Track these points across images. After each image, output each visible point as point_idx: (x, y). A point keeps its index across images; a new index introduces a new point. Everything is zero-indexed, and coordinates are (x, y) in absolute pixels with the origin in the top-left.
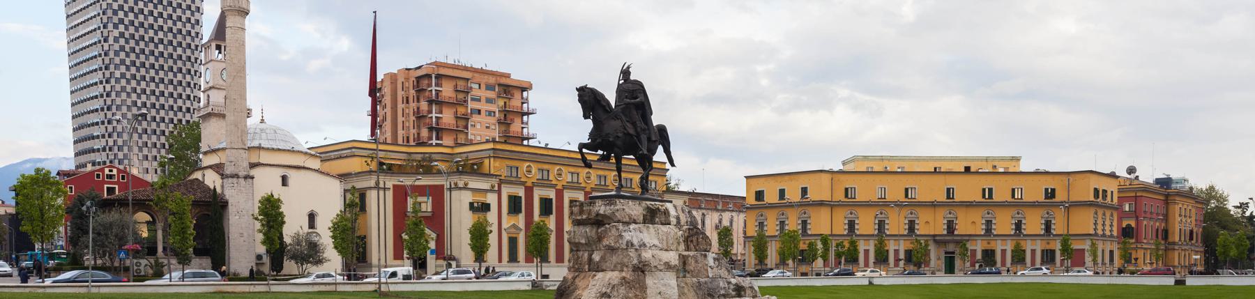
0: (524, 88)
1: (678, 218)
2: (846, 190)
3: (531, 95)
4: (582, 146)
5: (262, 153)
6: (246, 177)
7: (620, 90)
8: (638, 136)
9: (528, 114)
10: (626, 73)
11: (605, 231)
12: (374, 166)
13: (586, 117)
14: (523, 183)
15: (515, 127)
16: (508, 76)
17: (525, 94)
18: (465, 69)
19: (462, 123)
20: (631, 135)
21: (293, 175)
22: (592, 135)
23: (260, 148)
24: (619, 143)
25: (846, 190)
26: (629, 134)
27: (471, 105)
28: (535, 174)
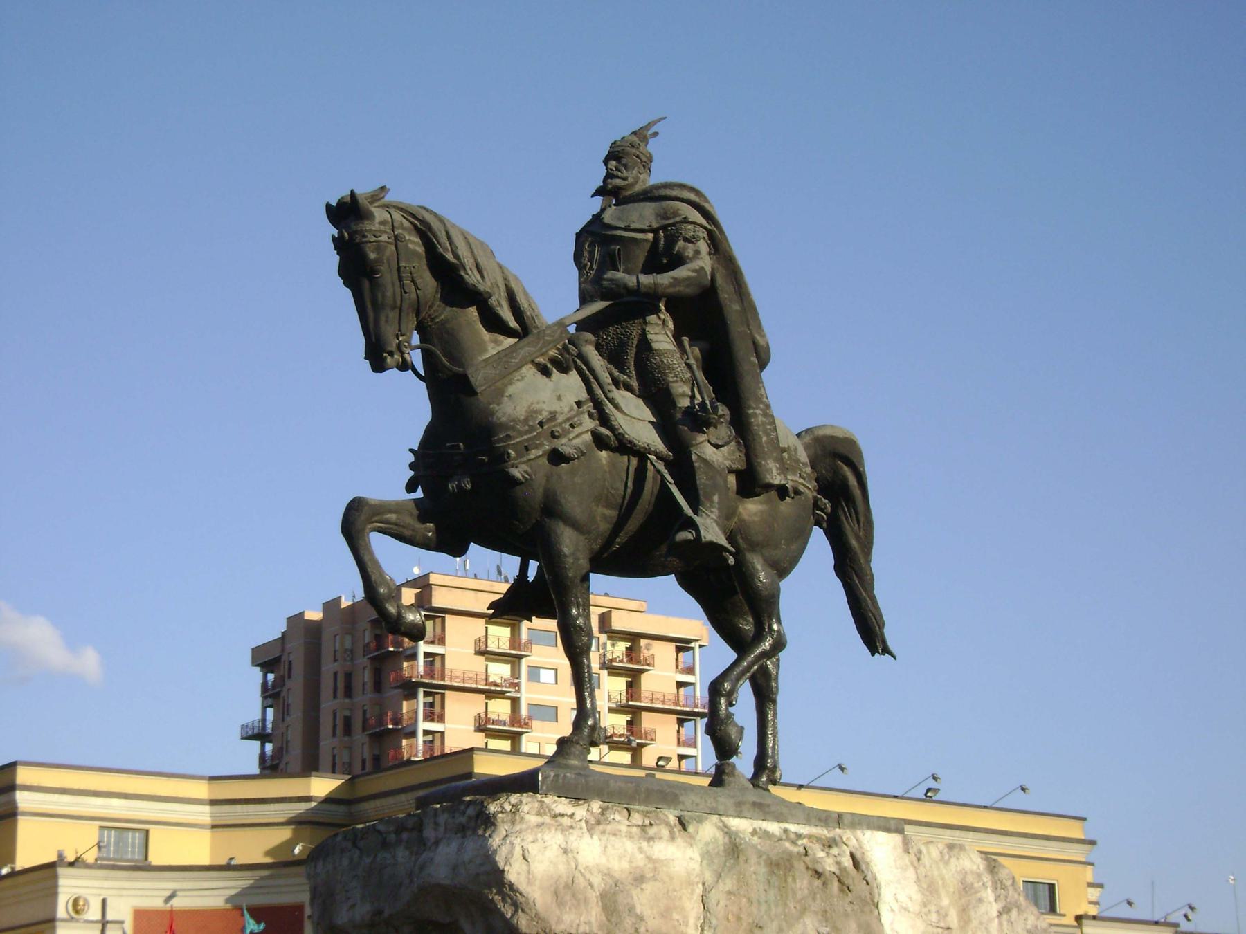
20: (641, 455)
22: (429, 463)
26: (624, 446)
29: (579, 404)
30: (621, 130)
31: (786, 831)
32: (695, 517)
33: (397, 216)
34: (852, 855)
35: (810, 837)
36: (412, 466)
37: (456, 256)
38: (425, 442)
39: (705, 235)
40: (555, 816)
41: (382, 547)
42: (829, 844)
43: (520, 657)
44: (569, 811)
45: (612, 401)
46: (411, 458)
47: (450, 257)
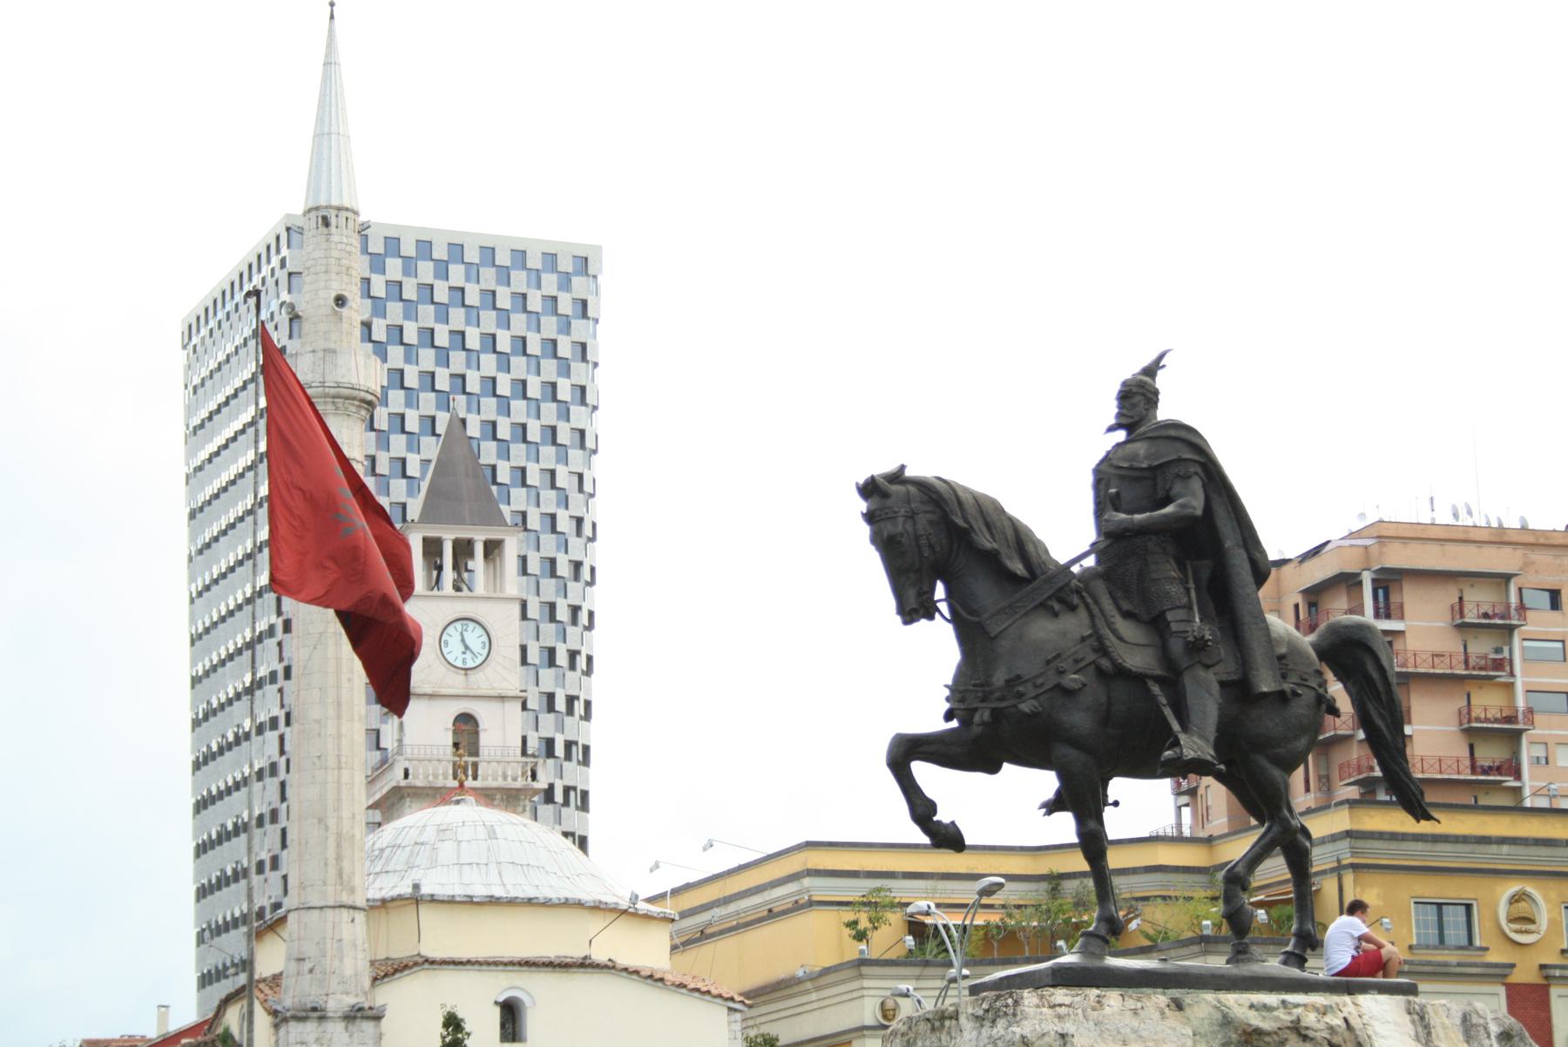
4: (906, 753)
5: (429, 917)
6: (355, 1015)
8: (1172, 680)
10: (1137, 398)
12: (890, 937)
13: (914, 608)
14: (1498, 973)
18: (1500, 538)
20: (1138, 679)
21: (536, 992)
22: (963, 695)
23: (416, 899)
24: (1079, 719)
26: (1122, 673)
29: (1083, 639)
30: (1130, 369)
31: (1283, 1002)
32: (1183, 738)
33: (912, 489)
34: (1346, 1020)
35: (1305, 1006)
36: (948, 699)
37: (967, 521)
38: (957, 679)
39: (1199, 470)
40: (1053, 1007)
41: (925, 773)
42: (1324, 1011)
43: (1510, 629)
44: (1067, 1000)
45: (1114, 632)
46: (947, 692)
47: (960, 522)
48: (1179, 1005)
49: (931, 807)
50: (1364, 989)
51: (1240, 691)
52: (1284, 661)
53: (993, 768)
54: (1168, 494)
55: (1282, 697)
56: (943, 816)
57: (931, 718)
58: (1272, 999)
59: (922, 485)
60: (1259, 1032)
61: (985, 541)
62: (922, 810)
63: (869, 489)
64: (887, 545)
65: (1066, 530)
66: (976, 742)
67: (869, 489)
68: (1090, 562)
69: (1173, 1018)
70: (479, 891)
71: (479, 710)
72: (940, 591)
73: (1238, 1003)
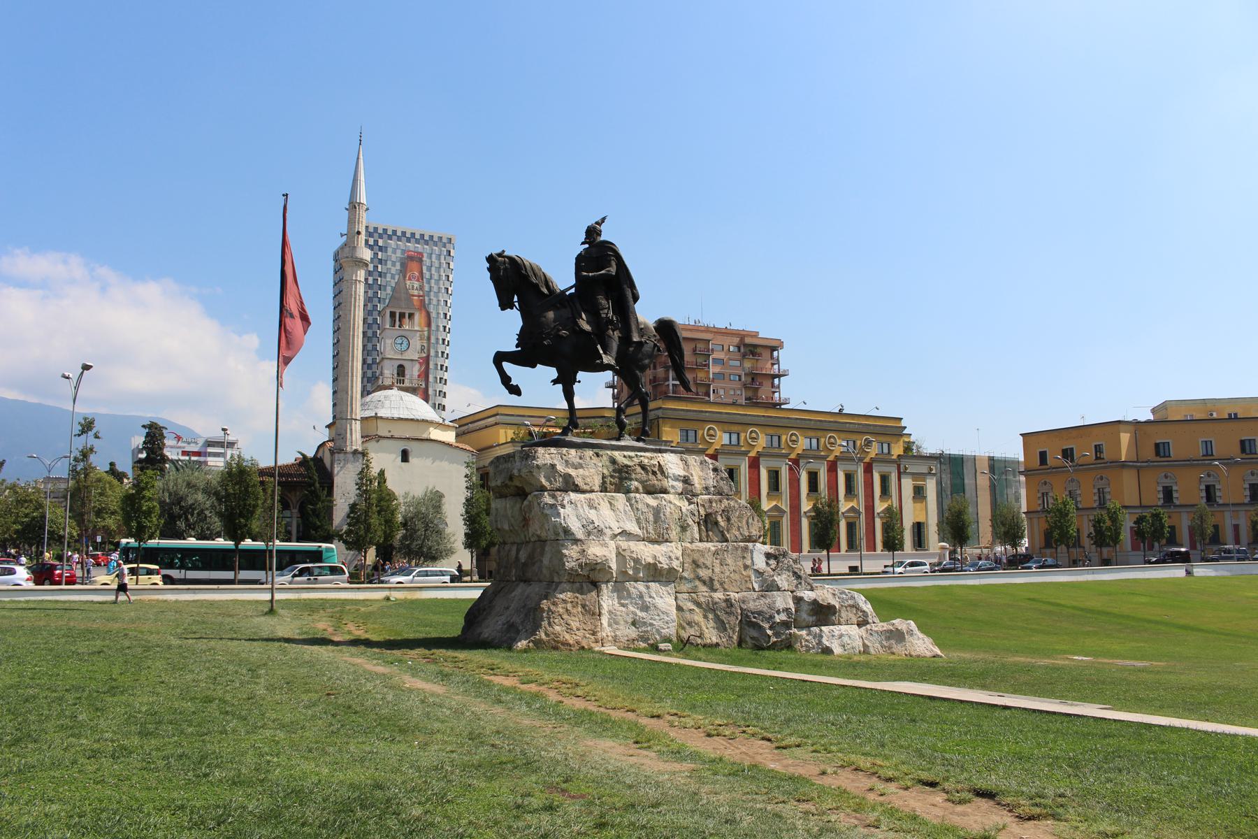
0: (773, 347)
1: (686, 480)
2: (1157, 445)
3: (782, 354)
4: (500, 358)
7: (582, 262)
9: (779, 376)
11: (530, 507)
13: (505, 304)
15: (763, 395)
16: (755, 335)
17: (775, 353)
18: (707, 329)
19: (702, 390)
22: (523, 337)
23: (376, 417)
25: (1157, 445)
27: (714, 369)
28: (762, 442)
30: (591, 222)
41: (507, 366)
42: (652, 458)
48: (598, 455)
49: (510, 379)
50: (666, 451)
51: (626, 339)
52: (642, 331)
53: (534, 366)
54: (603, 269)
55: (640, 344)
56: (513, 382)
57: (511, 345)
58: (632, 454)
59: (510, 258)
60: (627, 466)
61: (534, 280)
62: (506, 380)
63: (490, 259)
64: (494, 278)
65: (563, 278)
66: (527, 354)
67: (490, 259)
68: (573, 290)
69: (595, 460)
70: (396, 416)
71: (405, 364)
72: (516, 299)
73: (617, 455)
